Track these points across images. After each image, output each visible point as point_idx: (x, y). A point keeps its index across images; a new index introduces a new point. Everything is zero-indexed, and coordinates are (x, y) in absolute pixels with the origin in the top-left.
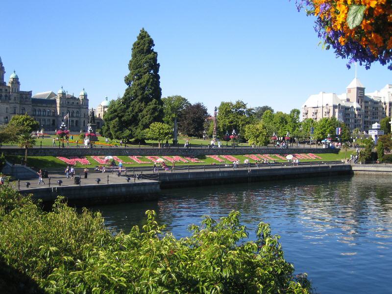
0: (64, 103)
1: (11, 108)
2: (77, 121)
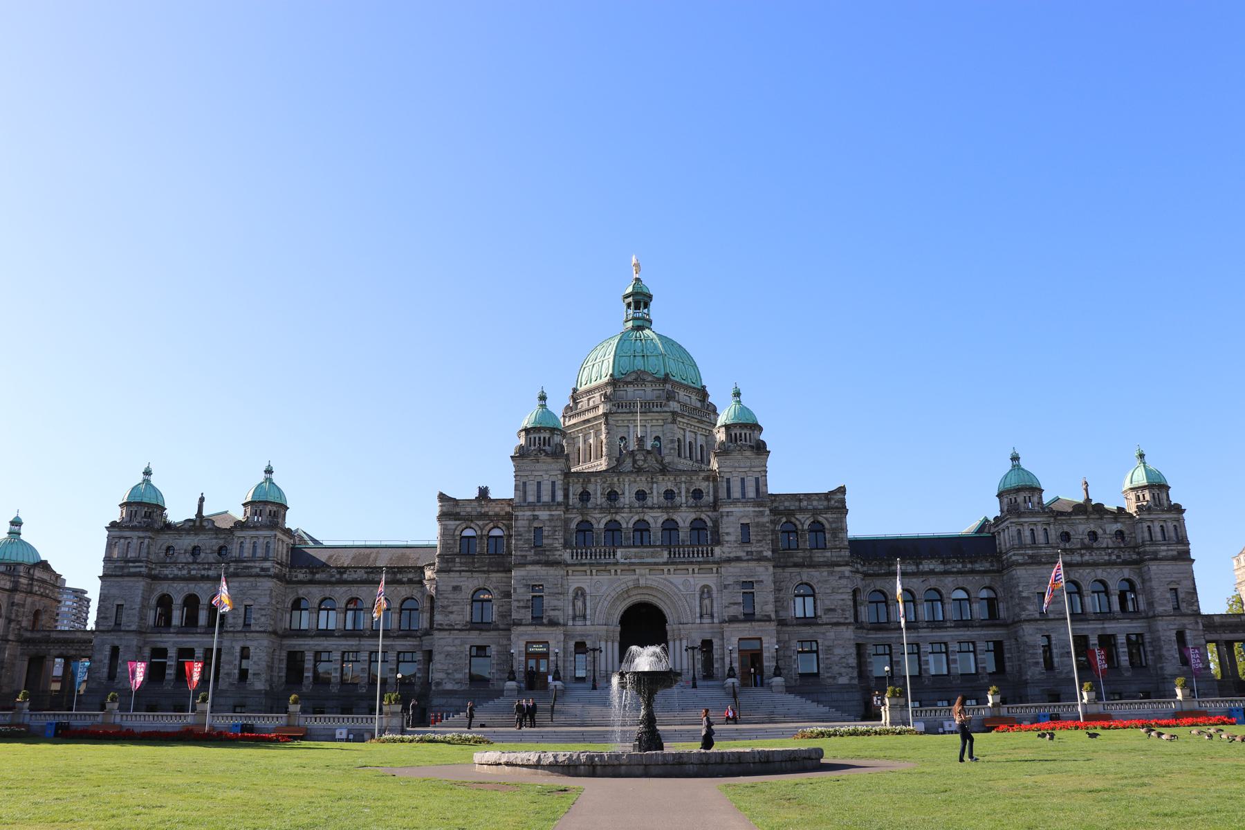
0: (1041, 538)
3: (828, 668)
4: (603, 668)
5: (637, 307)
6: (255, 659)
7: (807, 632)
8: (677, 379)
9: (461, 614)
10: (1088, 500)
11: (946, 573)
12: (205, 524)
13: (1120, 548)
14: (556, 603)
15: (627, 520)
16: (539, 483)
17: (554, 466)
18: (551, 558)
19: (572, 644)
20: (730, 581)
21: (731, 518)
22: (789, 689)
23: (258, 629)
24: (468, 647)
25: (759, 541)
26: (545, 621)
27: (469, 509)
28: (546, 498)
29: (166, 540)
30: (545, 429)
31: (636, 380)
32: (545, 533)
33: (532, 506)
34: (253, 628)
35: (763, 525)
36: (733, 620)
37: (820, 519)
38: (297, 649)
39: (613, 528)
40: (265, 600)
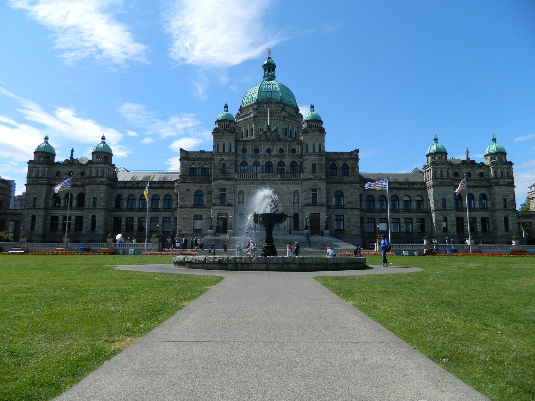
0: (445, 175)
2: (484, 221)
3: (348, 227)
5: (269, 71)
6: (99, 220)
7: (339, 212)
8: (286, 102)
9: (190, 201)
10: (468, 159)
11: (401, 189)
12: (74, 161)
13: (481, 180)
17: (231, 137)
18: (229, 177)
20: (307, 188)
21: (308, 161)
22: (332, 235)
23: (100, 207)
24: (193, 215)
26: (226, 204)
27: (194, 156)
28: (227, 151)
29: (58, 169)
30: (227, 120)
31: (268, 102)
32: (227, 166)
33: (221, 154)
34: (97, 207)
35: (322, 165)
36: (308, 205)
37: (347, 163)
38: (118, 216)
39: (256, 164)
40: (103, 195)
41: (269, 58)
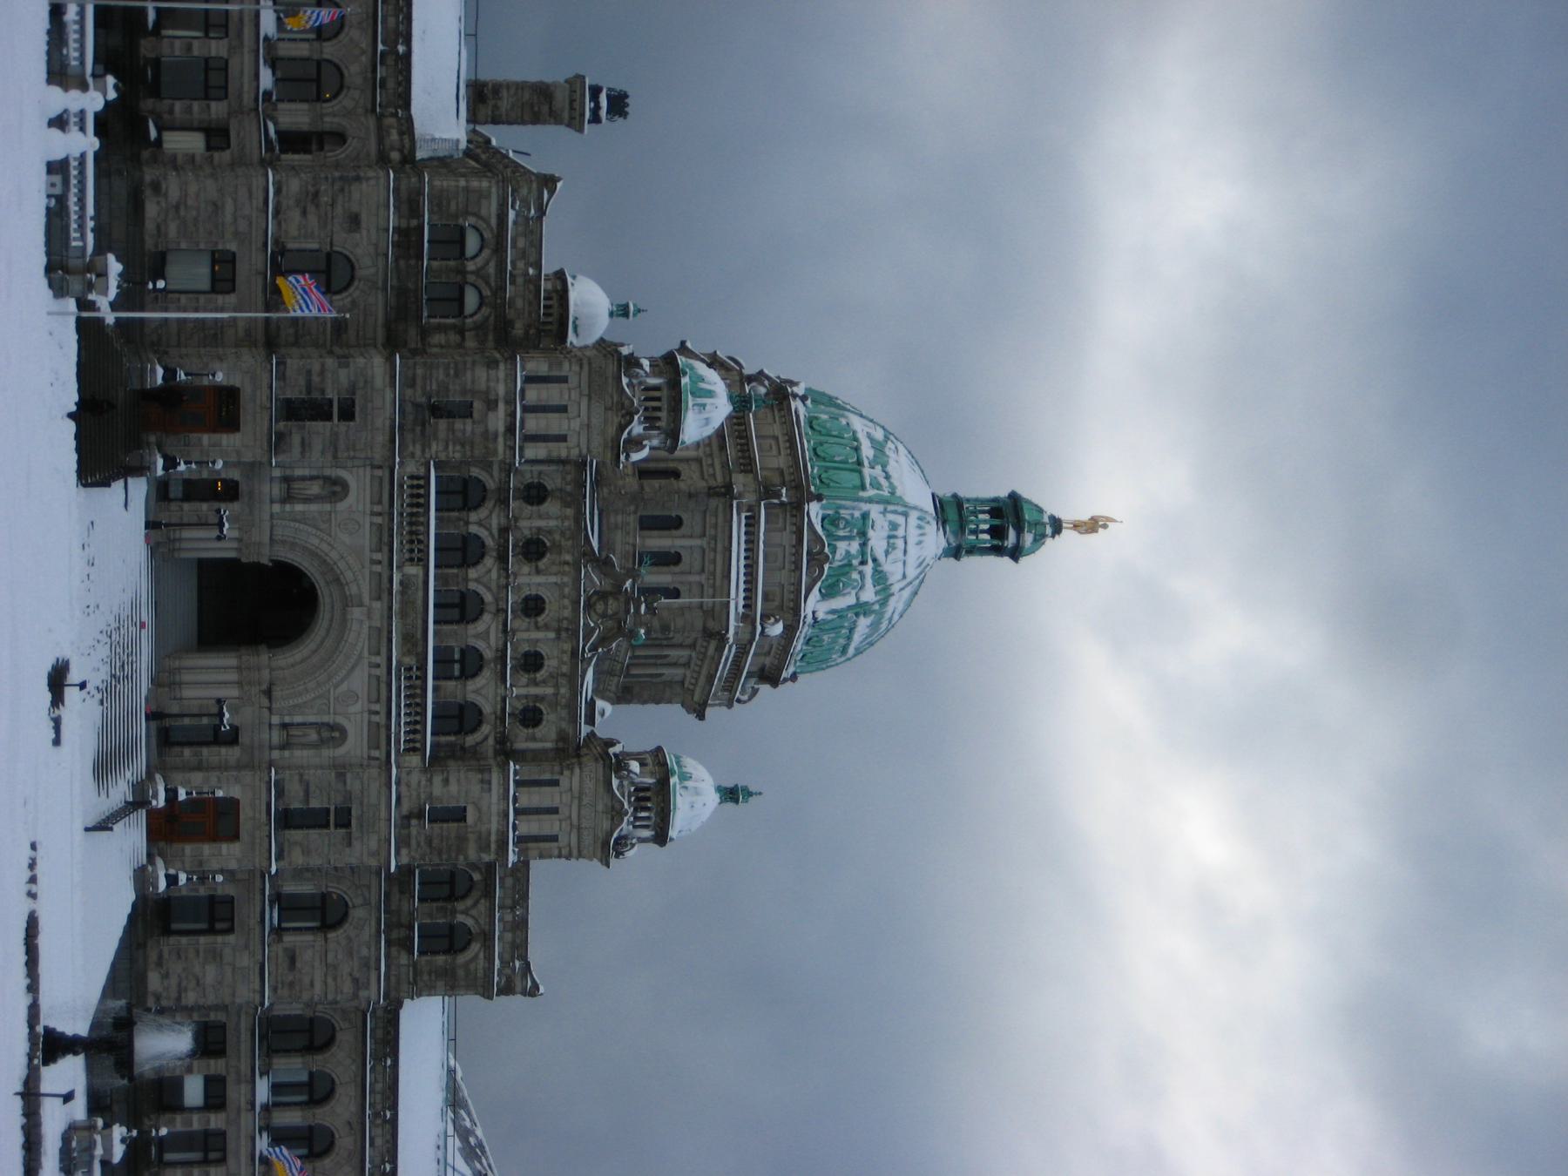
1: (341, 770)
4: (187, 534)
14: (317, 445)
15: (481, 578)
16: (563, 409)
17: (597, 442)
19: (235, 475)
20: (353, 784)
21: (476, 789)
25: (429, 841)
28: (534, 424)
32: (458, 424)
37: (475, 947)
41: (1057, 526)
